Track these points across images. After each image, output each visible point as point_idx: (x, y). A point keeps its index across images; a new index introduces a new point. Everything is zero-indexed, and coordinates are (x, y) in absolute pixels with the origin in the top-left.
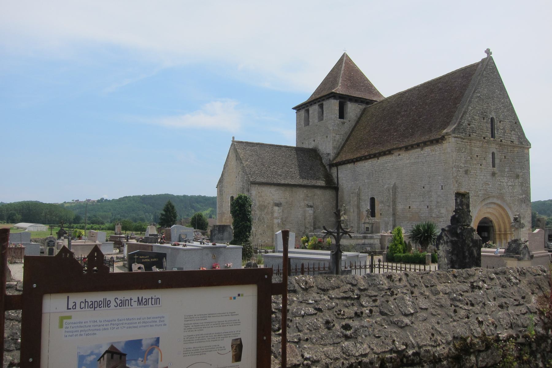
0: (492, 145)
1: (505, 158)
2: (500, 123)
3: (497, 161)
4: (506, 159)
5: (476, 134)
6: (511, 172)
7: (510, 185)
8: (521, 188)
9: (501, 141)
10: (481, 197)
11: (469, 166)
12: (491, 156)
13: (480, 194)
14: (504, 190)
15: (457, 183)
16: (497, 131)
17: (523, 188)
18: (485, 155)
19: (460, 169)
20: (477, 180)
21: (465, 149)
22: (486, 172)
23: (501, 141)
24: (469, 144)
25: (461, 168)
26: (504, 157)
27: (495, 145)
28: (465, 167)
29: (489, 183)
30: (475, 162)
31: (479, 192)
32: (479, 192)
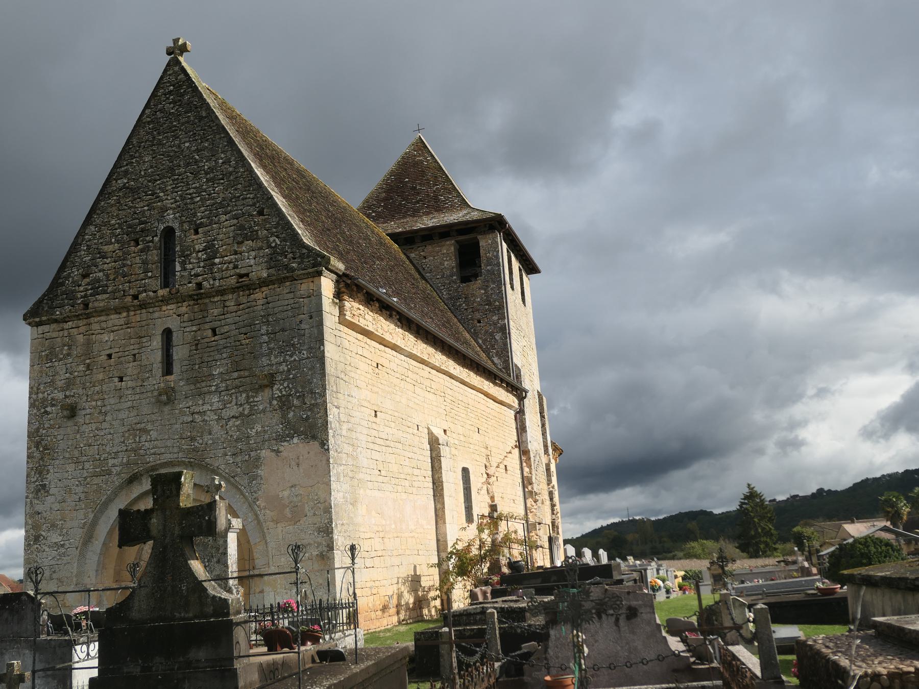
0: (164, 308)
1: (215, 334)
2: (197, 233)
3: (179, 353)
4: (216, 338)
5: (107, 296)
6: (235, 375)
7: (233, 417)
8: (284, 416)
9: (199, 286)
10: (118, 474)
11: (81, 391)
12: (157, 342)
13: (114, 465)
14: (206, 438)
15: (37, 448)
16: (183, 264)
17: (291, 415)
18: (137, 346)
19: (49, 409)
20: (105, 425)
21: (69, 349)
22: (137, 397)
23: (199, 286)
24: (83, 329)
25: (53, 405)
26: (210, 333)
27: (173, 306)
28: (66, 397)
29: (149, 427)
30: (101, 376)
31: (111, 462)
32: (111, 462)
